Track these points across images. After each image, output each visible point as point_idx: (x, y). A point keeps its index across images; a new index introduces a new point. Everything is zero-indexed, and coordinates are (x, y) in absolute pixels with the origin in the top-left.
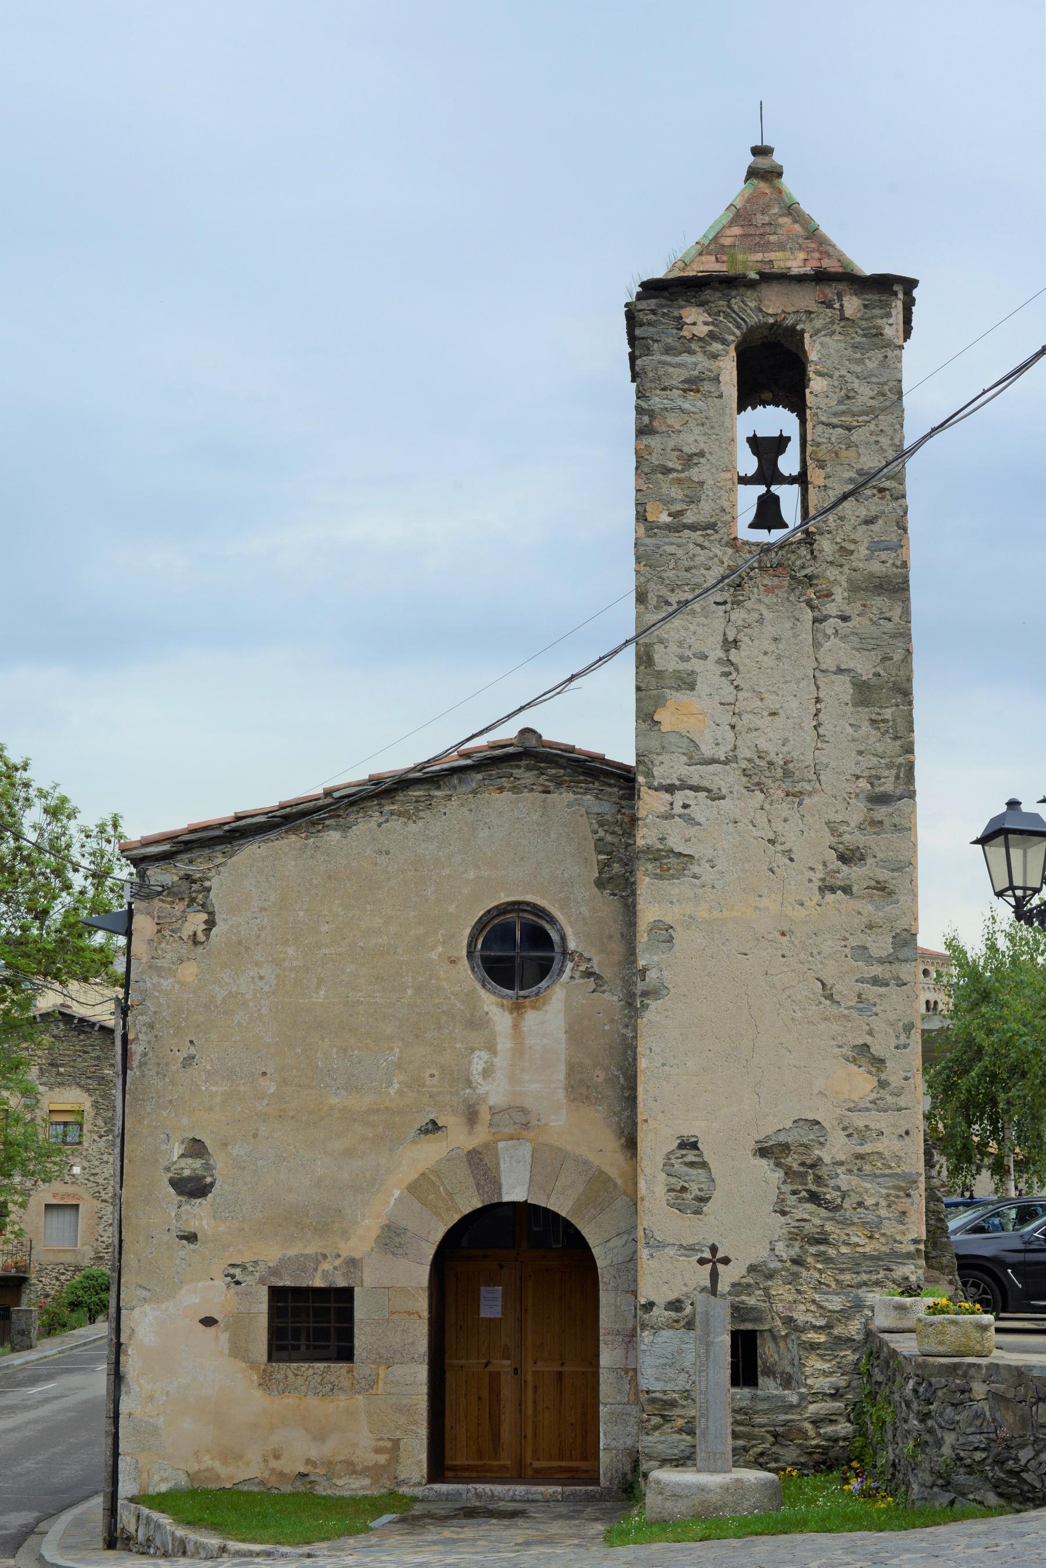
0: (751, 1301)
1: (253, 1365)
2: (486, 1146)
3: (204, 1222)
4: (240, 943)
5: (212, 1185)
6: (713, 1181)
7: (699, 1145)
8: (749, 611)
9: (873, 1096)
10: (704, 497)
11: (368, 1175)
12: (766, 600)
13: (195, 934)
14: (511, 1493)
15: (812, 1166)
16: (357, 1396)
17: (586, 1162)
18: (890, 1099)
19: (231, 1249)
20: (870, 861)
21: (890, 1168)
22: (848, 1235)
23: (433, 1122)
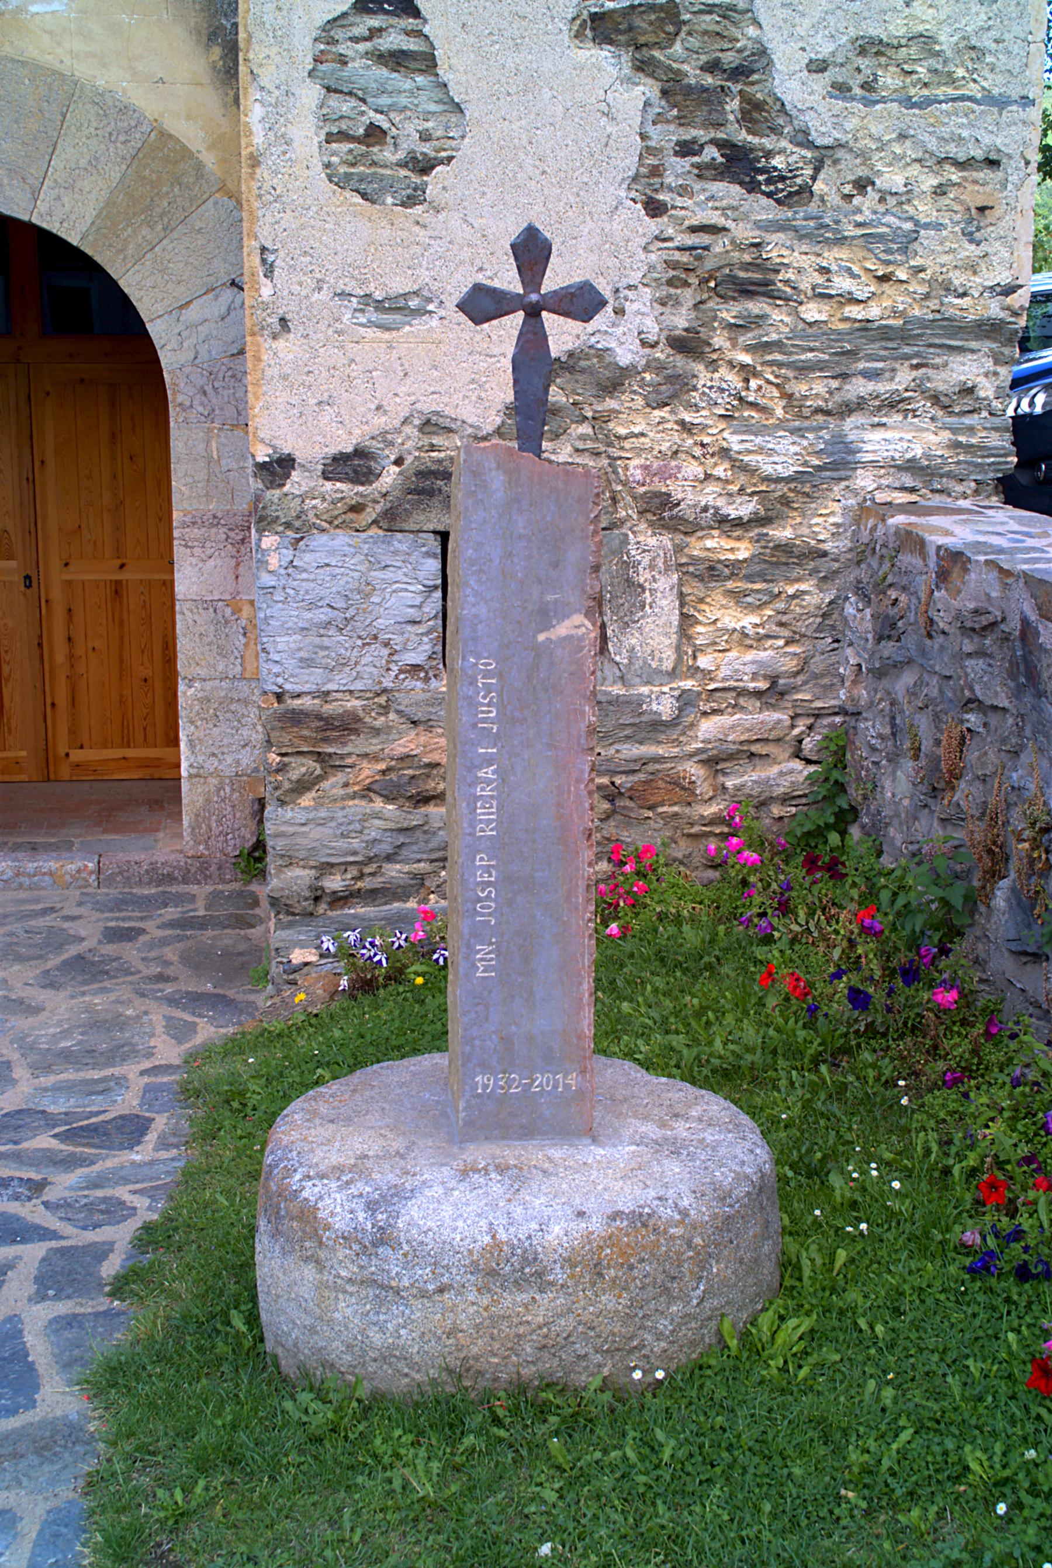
6: (458, 108)
15: (740, 73)
17: (124, 110)
21: (951, 80)
22: (824, 271)
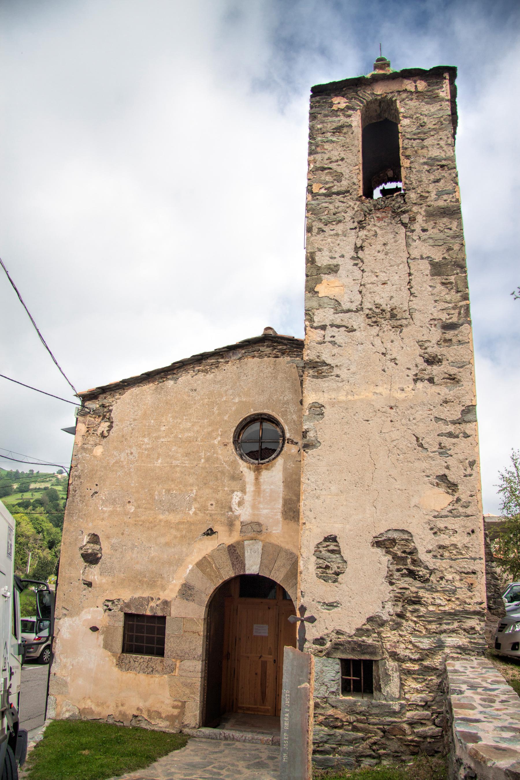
0: (370, 641)
1: (114, 654)
2: (238, 543)
3: (96, 577)
4: (123, 436)
5: (101, 558)
6: (345, 562)
7: (338, 539)
8: (369, 231)
9: (451, 507)
10: (343, 179)
11: (176, 557)
12: (378, 224)
13: (103, 432)
14: (244, 738)
15: (411, 553)
16: (165, 676)
17: (291, 553)
18: (461, 510)
19: (108, 592)
20: (444, 362)
21: (462, 554)
22: (433, 598)
23: (211, 529)
